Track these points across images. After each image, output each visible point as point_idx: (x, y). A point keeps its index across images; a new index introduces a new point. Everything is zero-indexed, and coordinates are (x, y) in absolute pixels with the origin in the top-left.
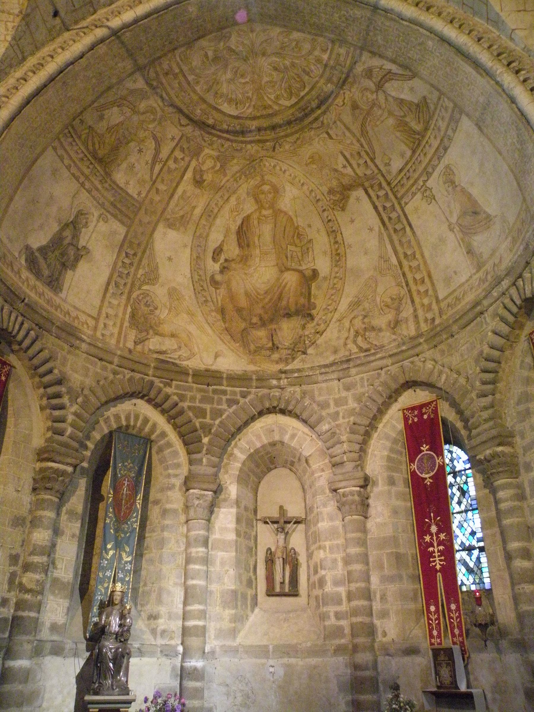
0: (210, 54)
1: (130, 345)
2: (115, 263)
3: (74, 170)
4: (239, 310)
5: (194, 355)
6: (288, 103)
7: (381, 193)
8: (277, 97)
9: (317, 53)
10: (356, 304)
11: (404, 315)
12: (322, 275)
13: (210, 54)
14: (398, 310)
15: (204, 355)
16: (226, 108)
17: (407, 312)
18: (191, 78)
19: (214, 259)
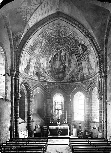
0: (51, 29)
1: (38, 79)
2: (35, 66)
3: (29, 53)
4: (53, 72)
5: (47, 79)
6: (64, 37)
7: (78, 56)
8: (62, 35)
9: (70, 31)
10: (72, 73)
11: (78, 76)
12: (67, 67)
13: (51, 29)
14: (78, 76)
15: (48, 79)
16: (53, 37)
17: (79, 76)
18: (47, 33)
19: (50, 63)
